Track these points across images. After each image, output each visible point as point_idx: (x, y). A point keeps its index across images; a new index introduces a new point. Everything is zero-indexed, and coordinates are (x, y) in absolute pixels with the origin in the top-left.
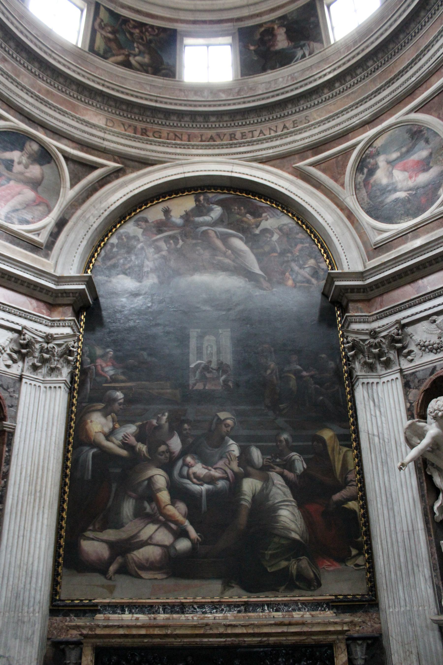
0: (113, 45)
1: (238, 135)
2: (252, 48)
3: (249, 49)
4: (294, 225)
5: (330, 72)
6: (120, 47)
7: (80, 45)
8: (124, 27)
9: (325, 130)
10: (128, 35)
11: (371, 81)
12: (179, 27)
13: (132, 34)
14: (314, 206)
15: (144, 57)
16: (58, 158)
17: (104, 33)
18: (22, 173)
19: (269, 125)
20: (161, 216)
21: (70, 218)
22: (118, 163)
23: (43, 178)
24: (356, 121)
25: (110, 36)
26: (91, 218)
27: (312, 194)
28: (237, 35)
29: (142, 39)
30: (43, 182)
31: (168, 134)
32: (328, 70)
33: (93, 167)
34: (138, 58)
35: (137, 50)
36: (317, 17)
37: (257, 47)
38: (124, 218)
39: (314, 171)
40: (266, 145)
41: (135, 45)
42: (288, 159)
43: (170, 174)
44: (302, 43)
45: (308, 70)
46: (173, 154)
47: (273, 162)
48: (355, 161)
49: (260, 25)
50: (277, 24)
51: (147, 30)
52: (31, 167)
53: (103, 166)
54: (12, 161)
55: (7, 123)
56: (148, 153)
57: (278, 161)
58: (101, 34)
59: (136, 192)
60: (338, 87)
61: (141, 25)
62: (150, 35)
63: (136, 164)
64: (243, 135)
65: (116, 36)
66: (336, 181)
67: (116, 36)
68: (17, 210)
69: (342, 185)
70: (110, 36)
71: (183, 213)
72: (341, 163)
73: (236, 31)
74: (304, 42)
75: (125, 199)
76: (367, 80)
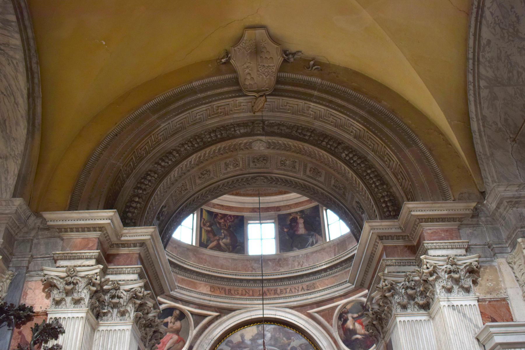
0: (211, 235)
1: (279, 291)
2: (285, 230)
3: (284, 231)
4: (308, 343)
5: (324, 265)
6: (215, 235)
7: (194, 244)
8: (215, 220)
9: (323, 296)
10: (218, 225)
11: (345, 272)
12: (246, 214)
13: (220, 223)
14: (317, 336)
15: (227, 239)
16: (188, 315)
17: (205, 228)
18: (171, 328)
19: (295, 286)
20: (240, 339)
21: (194, 345)
22: (217, 312)
23: (181, 327)
24: (337, 294)
25: (209, 229)
26: (205, 345)
27: (316, 329)
28: (277, 219)
29: (225, 225)
30: (181, 330)
31: (242, 291)
32: (324, 264)
33: (205, 316)
34: (224, 240)
35: (223, 234)
36: (319, 217)
37: (288, 229)
38: (221, 341)
39: (317, 315)
40: (293, 299)
41: (222, 231)
42: (304, 307)
43: (244, 317)
44: (312, 233)
45: (315, 253)
46: (245, 304)
47: (297, 309)
48: (337, 314)
49: (290, 214)
50: (299, 215)
51: (228, 219)
52: (176, 323)
53: (210, 315)
54: (167, 323)
55: (166, 305)
56: (232, 305)
57: (299, 308)
58: (205, 229)
59: (227, 328)
60: (329, 272)
61: (225, 216)
62: (230, 222)
63: (226, 311)
64: (281, 291)
65: (212, 228)
66: (328, 322)
67: (212, 228)
68: (171, 348)
69: (331, 325)
70: (209, 229)
71: (251, 338)
72: (331, 313)
73: (277, 216)
74: (314, 233)
75: (221, 333)
76: (343, 272)
